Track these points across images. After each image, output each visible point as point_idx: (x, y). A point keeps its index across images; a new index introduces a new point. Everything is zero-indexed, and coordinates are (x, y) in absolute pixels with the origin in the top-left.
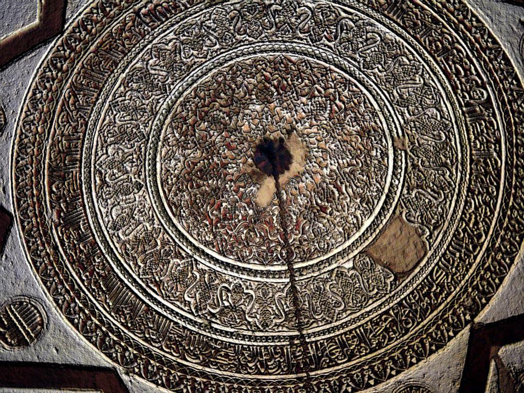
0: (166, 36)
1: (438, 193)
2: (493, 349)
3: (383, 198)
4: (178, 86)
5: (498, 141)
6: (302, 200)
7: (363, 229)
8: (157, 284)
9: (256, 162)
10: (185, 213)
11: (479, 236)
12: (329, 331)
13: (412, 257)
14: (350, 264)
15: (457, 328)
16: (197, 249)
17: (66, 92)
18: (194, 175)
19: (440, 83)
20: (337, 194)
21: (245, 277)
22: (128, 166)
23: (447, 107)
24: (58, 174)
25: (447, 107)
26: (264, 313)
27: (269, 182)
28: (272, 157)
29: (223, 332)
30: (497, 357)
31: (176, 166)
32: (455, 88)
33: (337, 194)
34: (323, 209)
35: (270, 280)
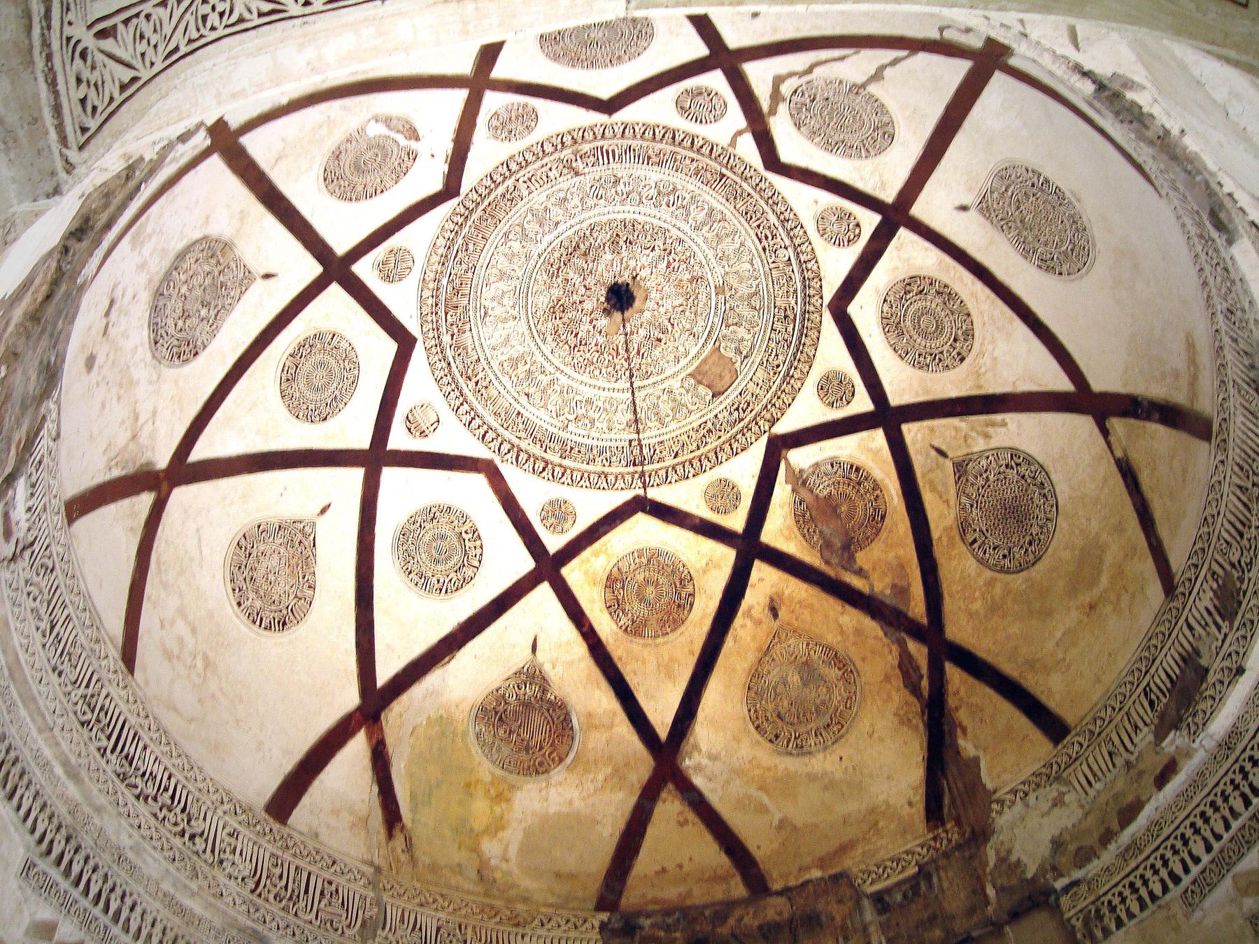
0: (539, 198)
2: (784, 452)
4: (548, 238)
5: (795, 291)
6: (642, 332)
7: (690, 357)
8: (527, 395)
9: (608, 300)
10: (549, 339)
11: (778, 366)
13: (727, 379)
14: (679, 384)
16: (558, 369)
17: (460, 241)
18: (557, 309)
19: (752, 244)
20: (670, 328)
21: (596, 391)
22: (505, 301)
23: (757, 261)
25: (757, 261)
27: (617, 316)
28: (620, 297)
29: (576, 434)
30: (787, 460)
31: (543, 301)
32: (764, 249)
33: (670, 328)
34: (660, 340)
35: (615, 395)
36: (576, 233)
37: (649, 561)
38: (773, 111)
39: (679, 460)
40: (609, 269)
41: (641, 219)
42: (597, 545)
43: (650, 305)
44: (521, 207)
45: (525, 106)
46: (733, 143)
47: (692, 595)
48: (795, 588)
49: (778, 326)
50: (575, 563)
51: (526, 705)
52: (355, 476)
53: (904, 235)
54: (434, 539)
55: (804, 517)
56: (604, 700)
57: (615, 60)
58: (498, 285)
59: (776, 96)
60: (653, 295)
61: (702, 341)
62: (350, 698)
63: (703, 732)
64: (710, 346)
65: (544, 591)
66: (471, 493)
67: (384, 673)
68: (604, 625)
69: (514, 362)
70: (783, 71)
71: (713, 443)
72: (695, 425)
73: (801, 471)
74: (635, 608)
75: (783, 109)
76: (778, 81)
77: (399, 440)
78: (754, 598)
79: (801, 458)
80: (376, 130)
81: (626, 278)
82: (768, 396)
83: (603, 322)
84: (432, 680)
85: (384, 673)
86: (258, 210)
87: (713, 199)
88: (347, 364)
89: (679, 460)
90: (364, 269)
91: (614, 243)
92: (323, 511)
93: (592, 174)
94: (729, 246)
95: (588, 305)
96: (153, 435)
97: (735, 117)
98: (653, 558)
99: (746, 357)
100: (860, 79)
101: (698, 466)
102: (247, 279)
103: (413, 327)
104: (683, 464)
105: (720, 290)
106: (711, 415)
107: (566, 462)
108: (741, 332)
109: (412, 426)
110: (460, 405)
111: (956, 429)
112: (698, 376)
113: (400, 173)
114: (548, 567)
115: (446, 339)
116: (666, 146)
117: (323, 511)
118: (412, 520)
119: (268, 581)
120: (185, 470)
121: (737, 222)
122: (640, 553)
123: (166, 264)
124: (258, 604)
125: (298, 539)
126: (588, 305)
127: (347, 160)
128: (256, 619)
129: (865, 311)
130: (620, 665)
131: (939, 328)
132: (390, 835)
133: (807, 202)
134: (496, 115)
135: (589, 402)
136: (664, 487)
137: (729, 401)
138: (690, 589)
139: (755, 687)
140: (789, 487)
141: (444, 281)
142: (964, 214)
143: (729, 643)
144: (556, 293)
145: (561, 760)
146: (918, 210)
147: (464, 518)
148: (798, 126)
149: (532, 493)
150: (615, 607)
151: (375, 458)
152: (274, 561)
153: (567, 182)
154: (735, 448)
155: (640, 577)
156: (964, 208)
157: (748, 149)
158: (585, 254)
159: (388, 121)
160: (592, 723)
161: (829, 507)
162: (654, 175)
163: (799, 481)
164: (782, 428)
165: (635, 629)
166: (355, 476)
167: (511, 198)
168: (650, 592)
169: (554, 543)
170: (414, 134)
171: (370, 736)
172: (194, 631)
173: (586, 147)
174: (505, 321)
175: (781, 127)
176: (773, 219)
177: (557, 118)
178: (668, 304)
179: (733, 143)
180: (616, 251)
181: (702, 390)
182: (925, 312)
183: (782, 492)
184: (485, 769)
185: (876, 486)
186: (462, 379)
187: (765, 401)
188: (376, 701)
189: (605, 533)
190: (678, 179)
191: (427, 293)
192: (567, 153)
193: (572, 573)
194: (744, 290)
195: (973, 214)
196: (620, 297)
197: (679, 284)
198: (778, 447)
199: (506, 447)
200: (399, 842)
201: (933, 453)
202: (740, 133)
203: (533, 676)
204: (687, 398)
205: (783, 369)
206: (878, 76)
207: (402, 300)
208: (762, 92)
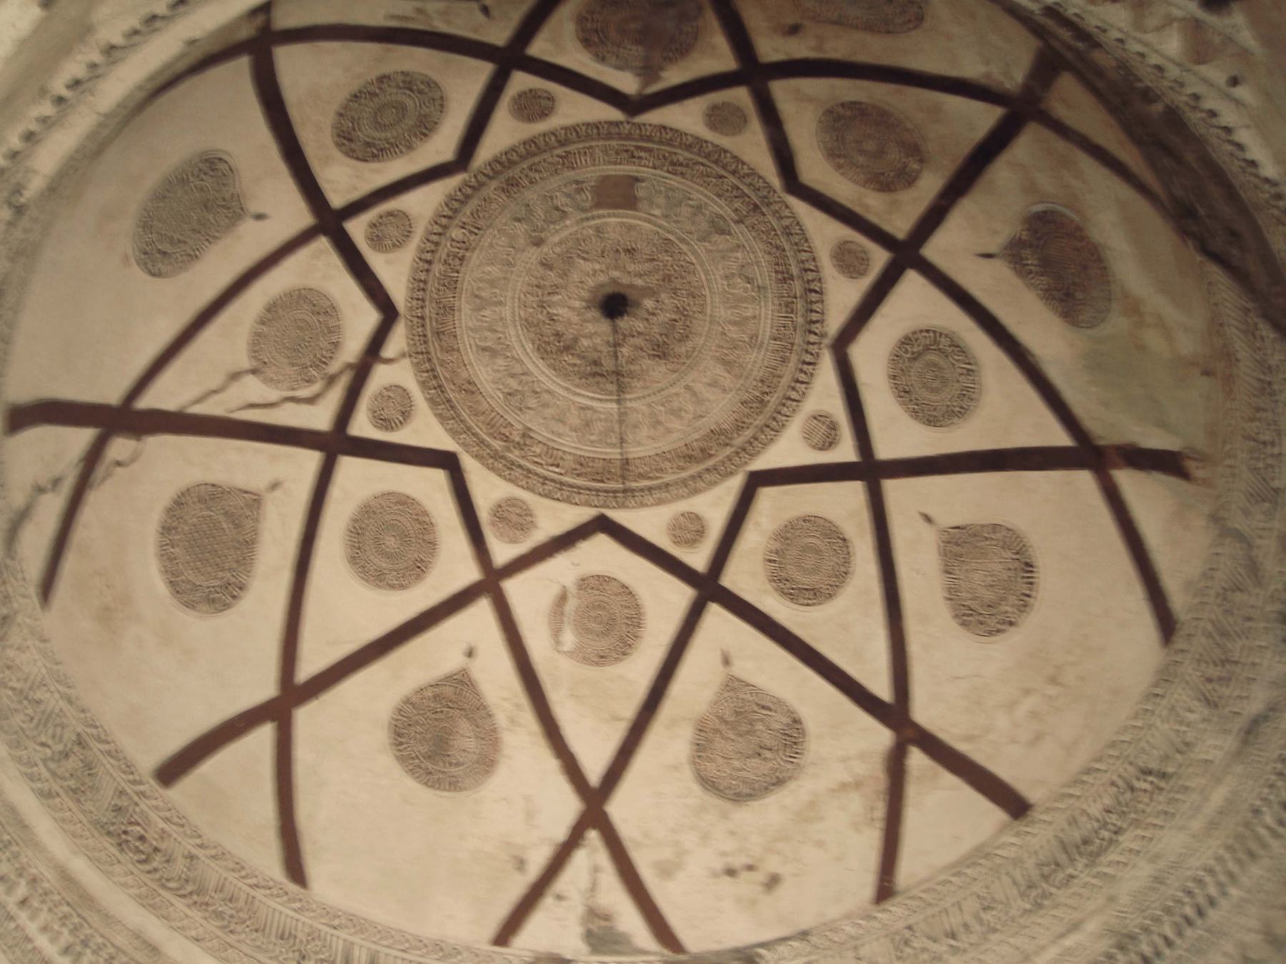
0: (569, 444)
1: (551, 198)
3: (585, 224)
6: (632, 267)
12: (713, 200)
15: (639, 126)
19: (474, 258)
24: (706, 454)
25: (486, 241)
26: (732, 251)
27: (632, 295)
28: (614, 305)
29: (764, 274)
36: (577, 386)
37: (839, 156)
38: (349, 366)
39: (722, 172)
40: (597, 330)
41: (529, 347)
42: (858, 210)
43: (602, 278)
44: (587, 451)
45: (493, 524)
46: (403, 355)
47: (843, 105)
48: (755, 21)
49: (525, 182)
50: (887, 227)
51: (1046, 265)
52: (893, 489)
53: (337, 200)
54: (925, 386)
55: (681, 49)
56: (1001, 172)
57: (404, 501)
58: (662, 419)
59: (331, 380)
60: (591, 282)
61: (598, 221)
62: (1084, 480)
63: (971, 69)
64: (595, 213)
65: (933, 251)
66: (871, 355)
67: (1060, 438)
68: (930, 185)
69: (727, 364)
70: (305, 409)
71: (683, 155)
72: (678, 178)
73: (638, 75)
74: (894, 155)
75: (334, 367)
76: (311, 400)
77: (846, 452)
78: (800, 49)
79: (627, 83)
80: (569, 638)
81: (594, 314)
82: (593, 144)
83: (649, 303)
84: (1055, 375)
85: (1060, 438)
86: (668, 709)
87: (465, 317)
88: (789, 534)
89: (722, 172)
90: (698, 559)
91: (567, 349)
92: (928, 519)
93: (518, 421)
94: (495, 271)
95: (640, 326)
96: (862, 756)
97: (381, 376)
98: (836, 155)
99: (577, 182)
100: (250, 380)
101: (718, 155)
102: (733, 685)
103: (735, 484)
104: (724, 167)
105: (538, 243)
106: (658, 172)
107: (795, 271)
108: (561, 200)
109: (829, 443)
110: (792, 401)
111: (448, 22)
112: (631, 203)
113: (603, 580)
114: (906, 255)
115: (739, 441)
116: (446, 392)
117: (928, 519)
118: (915, 414)
119: (996, 585)
120: (894, 713)
121: (470, 277)
122: (839, 167)
123: (712, 800)
124: (1013, 599)
125: (960, 544)
126: (640, 326)
127: (604, 644)
128: (1024, 605)
129: (442, 146)
130: (960, 160)
131: (381, 109)
132: (1183, 474)
133: (394, 271)
134: (514, 541)
135: (727, 277)
136: (762, 173)
137: (626, 167)
138: (840, 110)
139: (885, 28)
140: (664, 74)
141: (684, 474)
142: (261, 210)
143: (863, 58)
144: (647, 362)
145: (1079, 229)
146: (302, 217)
147: (896, 358)
148: (336, 345)
149: (843, 295)
150: (908, 179)
151: (870, 471)
152: (977, 577)
153: (541, 431)
154: (670, 136)
155: (861, 159)
156: (260, 217)
157: (397, 342)
158: (596, 363)
159: (556, 632)
160: (1030, 188)
161: (646, 37)
162: (484, 374)
163: (648, 72)
164: (614, 114)
165: (915, 151)
166: (893, 489)
167: (581, 465)
168: (870, 146)
169: (880, 257)
170: (563, 598)
171: (1117, 466)
172: (1027, 692)
173: (497, 444)
174: (694, 394)
175: (353, 346)
176: (437, 268)
177: (488, 489)
178: (588, 267)
179: (403, 355)
180: (576, 340)
181: (641, 193)
182: (380, 126)
183: (674, 76)
184: (1117, 323)
185: (581, 20)
186: (766, 408)
187: (601, 143)
188: (1087, 453)
189: (842, 207)
190: (471, 356)
191: (700, 484)
192: (514, 455)
193: (900, 226)
194: (521, 228)
195: (254, 207)
196: (614, 305)
197: (564, 275)
198: (631, 105)
199: (813, 338)
200: (1191, 465)
201: (495, 12)
202: (388, 361)
203: (1015, 253)
204: (661, 200)
205: (560, 151)
206: (235, 376)
207: (714, 505)
208: (334, 398)
